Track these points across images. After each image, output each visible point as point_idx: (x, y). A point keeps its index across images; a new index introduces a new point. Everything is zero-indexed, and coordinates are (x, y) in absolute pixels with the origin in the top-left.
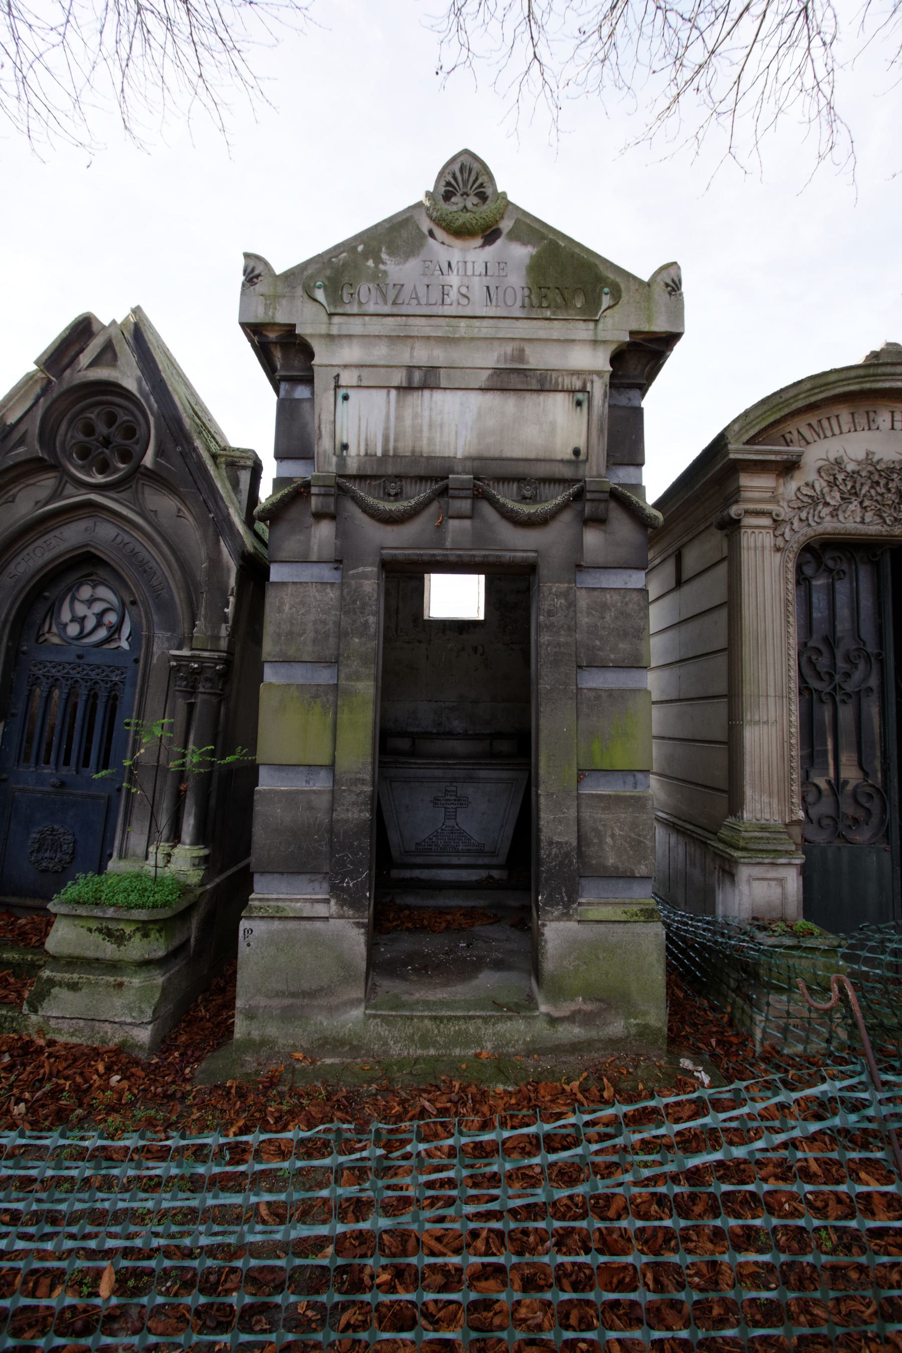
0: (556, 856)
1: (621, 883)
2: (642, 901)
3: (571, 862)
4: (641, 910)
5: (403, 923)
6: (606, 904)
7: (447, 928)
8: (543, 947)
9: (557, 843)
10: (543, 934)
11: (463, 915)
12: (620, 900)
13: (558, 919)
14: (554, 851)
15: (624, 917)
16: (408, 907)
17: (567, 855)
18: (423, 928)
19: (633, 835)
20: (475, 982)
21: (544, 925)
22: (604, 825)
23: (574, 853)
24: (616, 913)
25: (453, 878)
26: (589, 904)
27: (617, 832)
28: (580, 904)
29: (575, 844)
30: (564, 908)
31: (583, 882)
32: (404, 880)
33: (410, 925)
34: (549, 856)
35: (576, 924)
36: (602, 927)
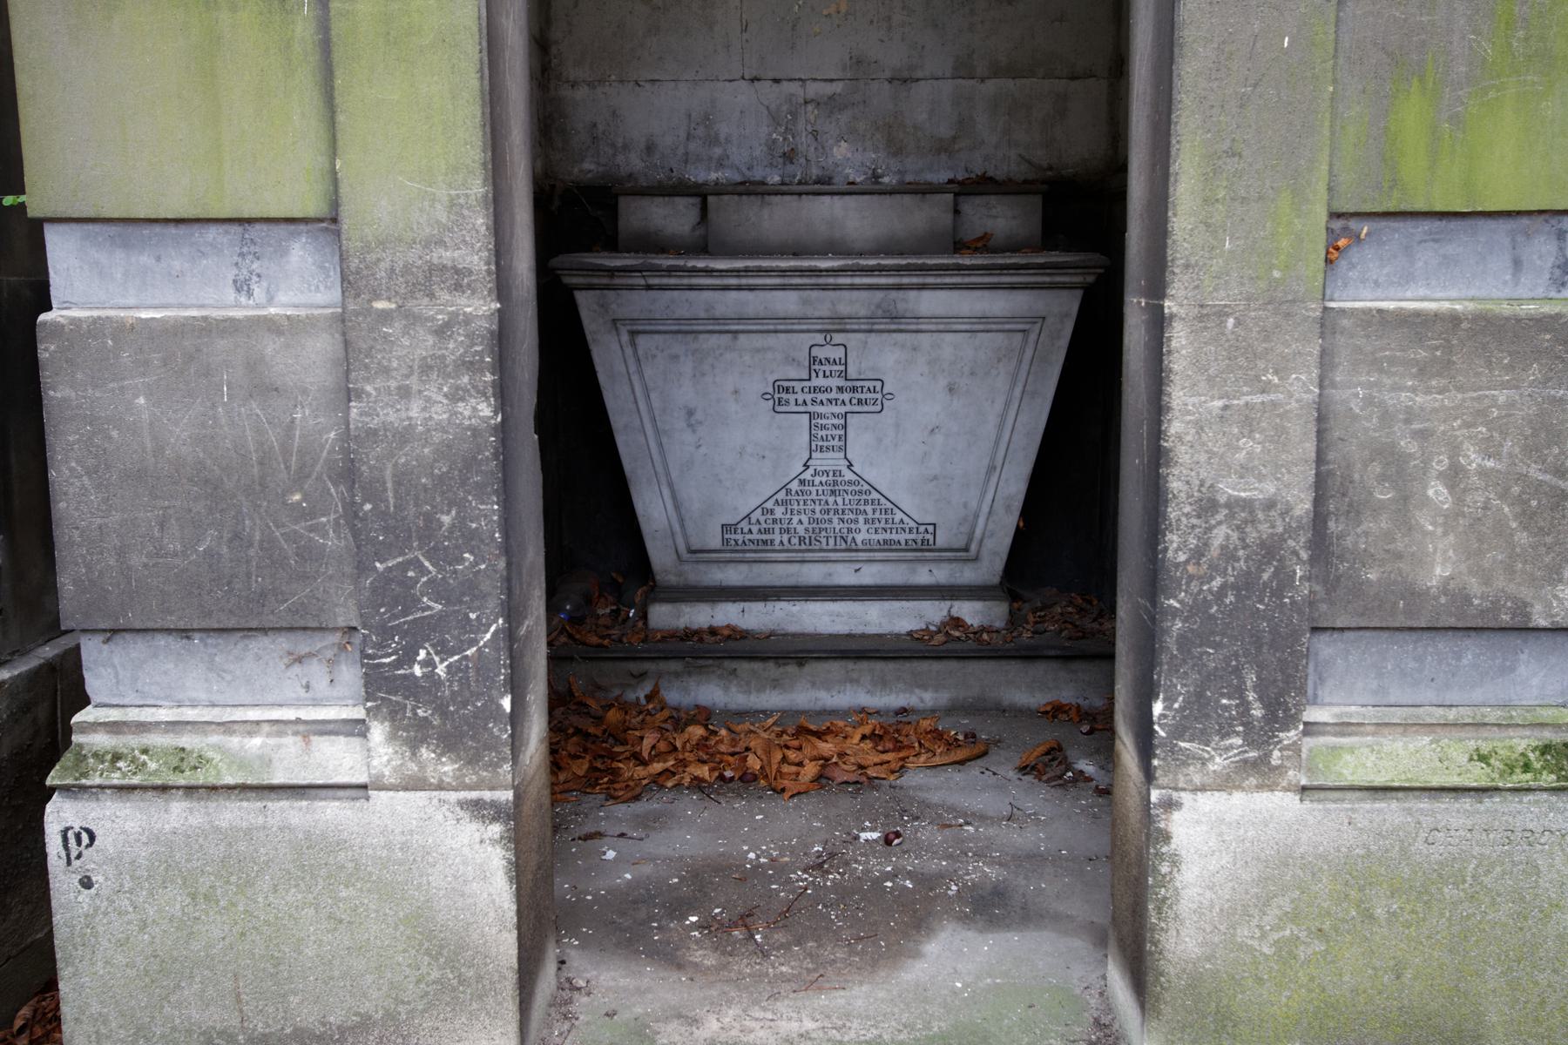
0: (1228, 554)
1: (1471, 652)
2: (1547, 714)
3: (1284, 580)
4: (1546, 749)
5: (683, 763)
6: (1406, 727)
7: (821, 779)
8: (1164, 881)
9: (1232, 504)
10: (1166, 837)
11: (874, 737)
12: (1466, 715)
13: (1225, 783)
14: (1220, 535)
15: (1477, 775)
16: (703, 715)
17: (1270, 550)
18: (747, 778)
19: (1535, 472)
20: (914, 972)
21: (1170, 805)
22: (1423, 435)
23: (1299, 545)
24: (1454, 761)
25: (840, 628)
26: (1343, 727)
27: (1473, 459)
28: (1311, 729)
29: (1303, 506)
30: (1250, 742)
31: (1325, 647)
32: (689, 634)
33: (704, 771)
34: (1198, 554)
35: (1292, 799)
36: (1391, 811)
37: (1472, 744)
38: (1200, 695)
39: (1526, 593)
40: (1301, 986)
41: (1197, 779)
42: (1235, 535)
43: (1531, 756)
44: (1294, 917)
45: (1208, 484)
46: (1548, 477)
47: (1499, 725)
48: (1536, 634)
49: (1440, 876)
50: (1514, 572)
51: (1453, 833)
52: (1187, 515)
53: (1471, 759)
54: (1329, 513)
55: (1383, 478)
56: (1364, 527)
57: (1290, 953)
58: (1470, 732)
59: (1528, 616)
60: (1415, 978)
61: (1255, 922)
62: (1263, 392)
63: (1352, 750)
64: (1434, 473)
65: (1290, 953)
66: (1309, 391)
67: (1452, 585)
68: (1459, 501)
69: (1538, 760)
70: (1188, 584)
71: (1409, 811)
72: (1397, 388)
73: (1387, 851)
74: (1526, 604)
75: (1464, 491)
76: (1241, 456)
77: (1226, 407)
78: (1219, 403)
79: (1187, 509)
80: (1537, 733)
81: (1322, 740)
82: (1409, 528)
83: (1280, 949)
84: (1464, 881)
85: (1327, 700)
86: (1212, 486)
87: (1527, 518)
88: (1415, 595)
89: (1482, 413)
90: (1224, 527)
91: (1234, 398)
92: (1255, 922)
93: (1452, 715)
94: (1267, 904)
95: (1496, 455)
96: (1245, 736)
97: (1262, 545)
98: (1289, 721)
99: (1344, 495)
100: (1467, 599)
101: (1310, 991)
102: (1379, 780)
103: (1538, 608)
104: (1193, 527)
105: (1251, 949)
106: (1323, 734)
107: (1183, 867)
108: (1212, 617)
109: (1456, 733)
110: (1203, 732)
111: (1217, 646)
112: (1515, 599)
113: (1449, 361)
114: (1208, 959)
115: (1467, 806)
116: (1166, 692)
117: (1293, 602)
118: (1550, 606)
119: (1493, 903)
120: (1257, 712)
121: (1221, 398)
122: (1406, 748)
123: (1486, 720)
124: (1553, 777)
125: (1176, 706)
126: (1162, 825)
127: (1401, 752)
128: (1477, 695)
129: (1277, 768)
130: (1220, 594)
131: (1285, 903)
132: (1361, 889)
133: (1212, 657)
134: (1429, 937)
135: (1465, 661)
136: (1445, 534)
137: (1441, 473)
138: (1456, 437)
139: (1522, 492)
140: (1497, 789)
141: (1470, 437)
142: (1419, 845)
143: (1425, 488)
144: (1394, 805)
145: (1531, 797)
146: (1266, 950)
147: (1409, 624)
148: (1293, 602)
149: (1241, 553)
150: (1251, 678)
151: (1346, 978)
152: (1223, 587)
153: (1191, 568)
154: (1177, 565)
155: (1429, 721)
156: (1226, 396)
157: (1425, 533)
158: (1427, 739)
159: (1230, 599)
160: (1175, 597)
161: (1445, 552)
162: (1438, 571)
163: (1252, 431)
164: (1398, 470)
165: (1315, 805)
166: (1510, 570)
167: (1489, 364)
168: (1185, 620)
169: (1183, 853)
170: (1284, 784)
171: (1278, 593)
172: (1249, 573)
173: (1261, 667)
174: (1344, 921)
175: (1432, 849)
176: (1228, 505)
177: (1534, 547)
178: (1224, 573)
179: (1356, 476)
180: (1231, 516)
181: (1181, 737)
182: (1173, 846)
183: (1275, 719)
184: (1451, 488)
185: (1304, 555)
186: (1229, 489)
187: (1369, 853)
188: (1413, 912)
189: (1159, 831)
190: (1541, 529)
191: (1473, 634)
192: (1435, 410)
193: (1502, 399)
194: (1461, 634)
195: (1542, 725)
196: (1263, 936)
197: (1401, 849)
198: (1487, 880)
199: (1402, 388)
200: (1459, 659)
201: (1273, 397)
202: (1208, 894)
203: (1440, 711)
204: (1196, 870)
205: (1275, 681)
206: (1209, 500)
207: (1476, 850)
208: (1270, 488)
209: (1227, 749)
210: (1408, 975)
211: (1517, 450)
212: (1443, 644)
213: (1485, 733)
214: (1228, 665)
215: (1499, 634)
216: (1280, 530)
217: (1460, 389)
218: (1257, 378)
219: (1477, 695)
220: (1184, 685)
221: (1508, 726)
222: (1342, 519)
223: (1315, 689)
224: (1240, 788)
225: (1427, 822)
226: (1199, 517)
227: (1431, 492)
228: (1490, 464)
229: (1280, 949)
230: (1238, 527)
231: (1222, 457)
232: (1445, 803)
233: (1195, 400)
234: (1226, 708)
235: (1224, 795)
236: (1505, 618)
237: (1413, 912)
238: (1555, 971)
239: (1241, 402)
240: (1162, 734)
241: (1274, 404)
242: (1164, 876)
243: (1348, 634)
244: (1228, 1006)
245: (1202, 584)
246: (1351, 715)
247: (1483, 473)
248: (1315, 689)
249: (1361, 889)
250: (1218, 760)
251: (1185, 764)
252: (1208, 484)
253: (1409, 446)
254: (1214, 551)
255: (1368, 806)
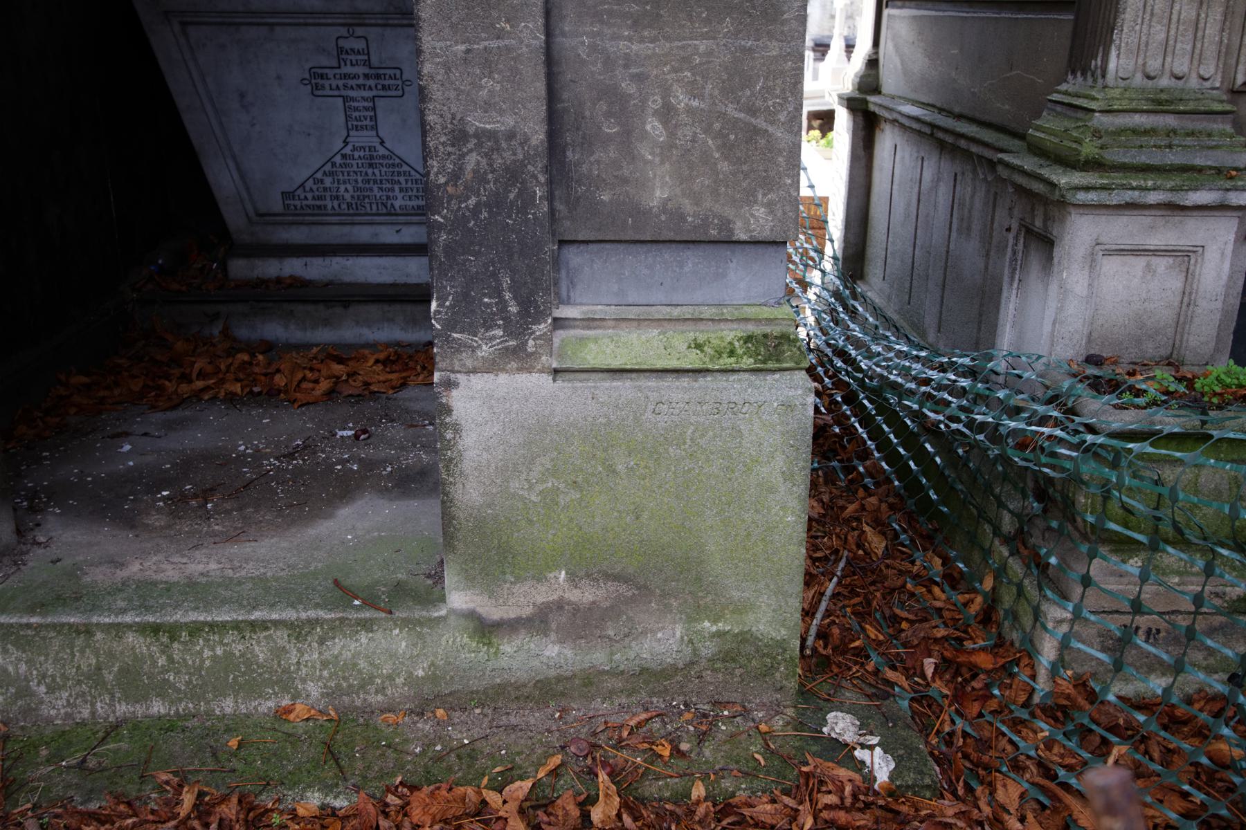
0: (480, 177)
1: (692, 260)
2: (750, 312)
3: (527, 200)
4: (748, 339)
5: (222, 381)
6: (639, 321)
8: (449, 445)
9: (481, 135)
10: (448, 410)
11: (385, 362)
12: (687, 312)
13: (491, 367)
14: (472, 160)
15: (693, 360)
16: (268, 347)
17: (513, 174)
18: (272, 393)
19: (732, 111)
20: (322, 528)
21: (450, 384)
22: (640, 78)
23: (537, 169)
24: (674, 348)
25: (386, 278)
26: (590, 322)
27: (681, 99)
28: (559, 323)
29: (538, 136)
30: (509, 333)
31: (574, 257)
32: (263, 283)
33: (237, 388)
34: (455, 177)
35: (546, 379)
36: (625, 388)
37: (691, 335)
38: (466, 295)
39: (729, 212)
40: (563, 526)
41: (469, 363)
42: (484, 161)
43: (737, 344)
44: (554, 473)
45: (458, 117)
46: (742, 115)
47: (712, 320)
48: (741, 246)
49: (666, 439)
50: (719, 195)
51: (674, 405)
52: (443, 144)
53: (689, 347)
54: (567, 145)
55: (609, 114)
56: (595, 156)
57: (553, 500)
58: (690, 326)
59: (731, 231)
60: (650, 518)
61: (524, 476)
62: (498, 38)
63: (596, 340)
64: (650, 111)
65: (553, 500)
66: (536, 38)
67: (669, 206)
68: (672, 135)
69: (741, 347)
70: (448, 202)
71: (639, 389)
72: (616, 37)
73: (623, 420)
74: (729, 222)
75: (676, 126)
76: (484, 93)
77: (468, 51)
78: (462, 47)
79: (443, 139)
80: (742, 326)
81: (572, 332)
82: (633, 157)
83: (545, 498)
84: (685, 443)
85: (578, 300)
86: (461, 119)
87: (727, 149)
88: (641, 213)
89: (686, 60)
90: (474, 154)
91: (475, 43)
92: (524, 476)
93: (676, 312)
94: (532, 461)
95: (700, 96)
96: (505, 328)
97: (507, 169)
98: (539, 317)
99: (578, 129)
100: (682, 217)
101: (570, 529)
102: (615, 364)
103: (739, 224)
104: (449, 154)
105: (522, 498)
106: (574, 327)
107: (464, 434)
108: (470, 230)
109: (680, 327)
110: (471, 324)
111: (477, 254)
112: (720, 218)
113: (658, 14)
114: (489, 506)
115: (685, 384)
116: (438, 292)
117: (536, 218)
118: (748, 223)
119: (708, 460)
120: (513, 309)
121: (463, 43)
122: (639, 338)
123: (702, 316)
124: (752, 360)
125: (447, 303)
126: (444, 401)
127: (635, 341)
128: (698, 297)
129: (532, 354)
130: (476, 211)
131: (546, 461)
132: (605, 450)
133: (473, 264)
134: (660, 487)
135: (686, 269)
136: (662, 162)
137: (656, 111)
138: (667, 81)
139: (723, 128)
140: (708, 370)
141: (678, 81)
142: (649, 414)
143: (644, 123)
144: (628, 383)
145: (735, 377)
146: (533, 498)
147: (637, 237)
148: (536, 218)
149: (490, 176)
150: (506, 281)
151: (597, 520)
152: (477, 205)
153: (449, 189)
154: (439, 186)
155: (657, 316)
156: (467, 41)
157: (646, 162)
158: (656, 331)
159: (484, 215)
160: (439, 214)
161: (663, 177)
162: (658, 193)
163: (491, 72)
164: (621, 107)
165: (566, 384)
166: (715, 193)
167: (690, 18)
168: (449, 233)
169: (463, 422)
170: (539, 367)
171: (523, 210)
172: (498, 193)
173: (513, 272)
174: (593, 475)
175: (659, 418)
176: (476, 135)
177: (734, 174)
178: (478, 194)
179: (587, 113)
180: (479, 145)
181: (454, 330)
182: (454, 417)
183: (528, 314)
184: (665, 123)
185: (542, 179)
186: (476, 121)
187: (609, 422)
188: (646, 467)
189: (442, 404)
190: (739, 159)
191: (691, 246)
192: (648, 57)
193: (702, 48)
194: (682, 246)
195: (746, 320)
196: (531, 488)
197: (635, 418)
198: (702, 442)
199: (620, 38)
200: (681, 267)
201: (507, 42)
202: (485, 455)
203: (668, 309)
204: (474, 436)
205: (526, 283)
206: (460, 131)
207: (693, 419)
208: (510, 121)
209: (492, 338)
210: (645, 516)
211: (716, 92)
212: (667, 254)
213: (701, 326)
214: (487, 270)
215: (712, 246)
216: (521, 157)
217: (668, 38)
218: (493, 25)
219: (698, 297)
220: (452, 287)
221: (720, 320)
222: (578, 149)
223: (568, 291)
224: (503, 370)
225: (654, 396)
226: (453, 145)
227: (648, 127)
228: (695, 103)
229: (545, 498)
230: (486, 155)
231: (468, 95)
232: (669, 382)
233: (442, 44)
234: (488, 305)
235: (492, 376)
236: (713, 233)
237: (646, 467)
238: (757, 511)
239: (481, 47)
240: (438, 327)
241: (508, 49)
242: (449, 441)
243: (591, 246)
244: (507, 542)
245: (460, 202)
246: (595, 312)
247: (690, 111)
248: (568, 291)
249: (605, 450)
250: (484, 348)
251: (458, 351)
252: (458, 117)
253: (629, 87)
254: (468, 175)
255: (607, 384)
